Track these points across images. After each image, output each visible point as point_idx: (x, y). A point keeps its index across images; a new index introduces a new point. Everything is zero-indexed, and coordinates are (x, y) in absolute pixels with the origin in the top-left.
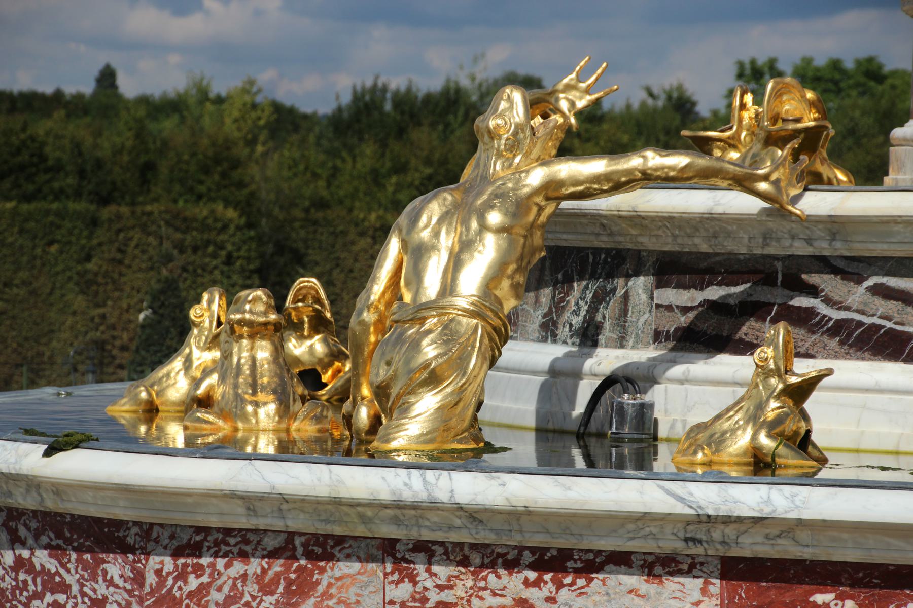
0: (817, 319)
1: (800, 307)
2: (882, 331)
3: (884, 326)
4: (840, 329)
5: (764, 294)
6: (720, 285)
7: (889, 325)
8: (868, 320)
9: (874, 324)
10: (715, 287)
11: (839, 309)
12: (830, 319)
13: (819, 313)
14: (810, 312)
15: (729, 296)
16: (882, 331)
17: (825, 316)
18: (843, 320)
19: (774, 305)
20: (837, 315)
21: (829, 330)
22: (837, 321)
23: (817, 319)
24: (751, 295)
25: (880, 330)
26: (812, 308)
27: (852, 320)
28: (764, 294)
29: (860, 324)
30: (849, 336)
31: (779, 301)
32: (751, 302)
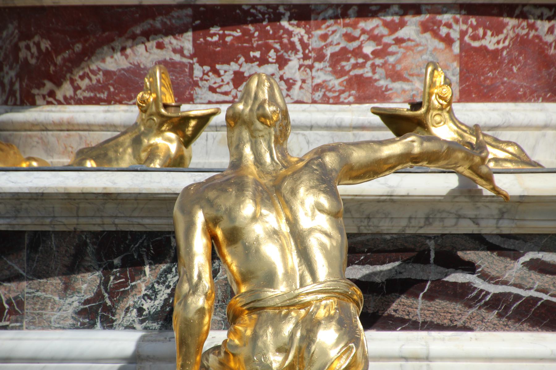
0: (474, 294)
1: (455, 283)
2: (540, 303)
3: (541, 299)
4: (497, 303)
5: (415, 272)
6: (363, 264)
7: (546, 297)
8: (525, 294)
9: (531, 297)
10: (357, 266)
11: (497, 283)
12: (488, 293)
13: (475, 288)
14: (467, 287)
15: (375, 274)
16: (540, 303)
17: (482, 291)
18: (501, 294)
19: (427, 281)
20: (494, 289)
21: (486, 303)
22: (495, 295)
23: (474, 294)
24: (400, 273)
25: (537, 302)
26: (469, 283)
27: (510, 294)
28: (415, 272)
29: (518, 297)
30: (507, 308)
31: (433, 277)
32: (400, 279)
